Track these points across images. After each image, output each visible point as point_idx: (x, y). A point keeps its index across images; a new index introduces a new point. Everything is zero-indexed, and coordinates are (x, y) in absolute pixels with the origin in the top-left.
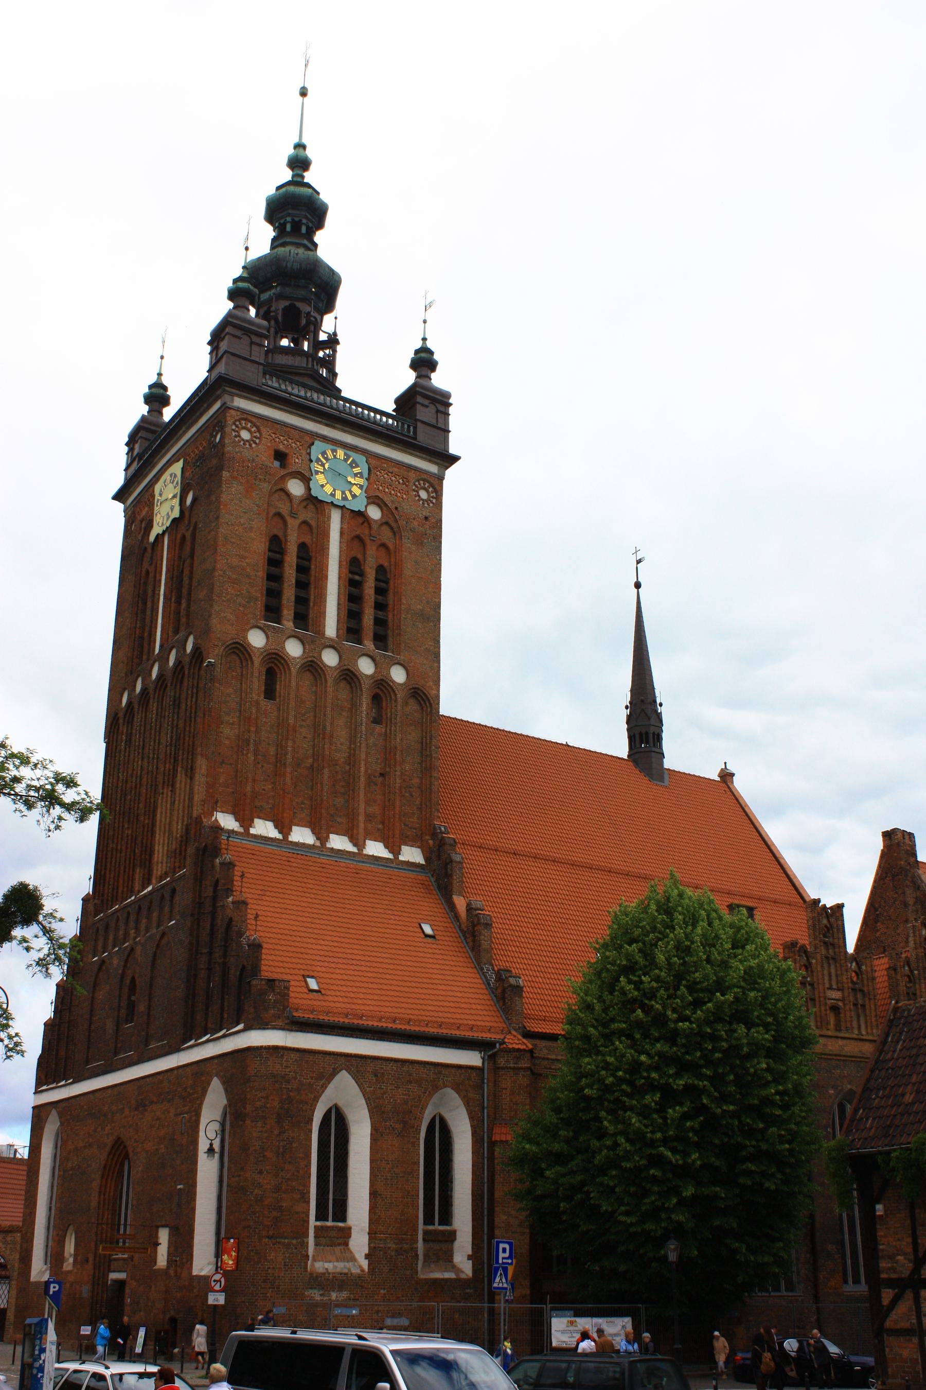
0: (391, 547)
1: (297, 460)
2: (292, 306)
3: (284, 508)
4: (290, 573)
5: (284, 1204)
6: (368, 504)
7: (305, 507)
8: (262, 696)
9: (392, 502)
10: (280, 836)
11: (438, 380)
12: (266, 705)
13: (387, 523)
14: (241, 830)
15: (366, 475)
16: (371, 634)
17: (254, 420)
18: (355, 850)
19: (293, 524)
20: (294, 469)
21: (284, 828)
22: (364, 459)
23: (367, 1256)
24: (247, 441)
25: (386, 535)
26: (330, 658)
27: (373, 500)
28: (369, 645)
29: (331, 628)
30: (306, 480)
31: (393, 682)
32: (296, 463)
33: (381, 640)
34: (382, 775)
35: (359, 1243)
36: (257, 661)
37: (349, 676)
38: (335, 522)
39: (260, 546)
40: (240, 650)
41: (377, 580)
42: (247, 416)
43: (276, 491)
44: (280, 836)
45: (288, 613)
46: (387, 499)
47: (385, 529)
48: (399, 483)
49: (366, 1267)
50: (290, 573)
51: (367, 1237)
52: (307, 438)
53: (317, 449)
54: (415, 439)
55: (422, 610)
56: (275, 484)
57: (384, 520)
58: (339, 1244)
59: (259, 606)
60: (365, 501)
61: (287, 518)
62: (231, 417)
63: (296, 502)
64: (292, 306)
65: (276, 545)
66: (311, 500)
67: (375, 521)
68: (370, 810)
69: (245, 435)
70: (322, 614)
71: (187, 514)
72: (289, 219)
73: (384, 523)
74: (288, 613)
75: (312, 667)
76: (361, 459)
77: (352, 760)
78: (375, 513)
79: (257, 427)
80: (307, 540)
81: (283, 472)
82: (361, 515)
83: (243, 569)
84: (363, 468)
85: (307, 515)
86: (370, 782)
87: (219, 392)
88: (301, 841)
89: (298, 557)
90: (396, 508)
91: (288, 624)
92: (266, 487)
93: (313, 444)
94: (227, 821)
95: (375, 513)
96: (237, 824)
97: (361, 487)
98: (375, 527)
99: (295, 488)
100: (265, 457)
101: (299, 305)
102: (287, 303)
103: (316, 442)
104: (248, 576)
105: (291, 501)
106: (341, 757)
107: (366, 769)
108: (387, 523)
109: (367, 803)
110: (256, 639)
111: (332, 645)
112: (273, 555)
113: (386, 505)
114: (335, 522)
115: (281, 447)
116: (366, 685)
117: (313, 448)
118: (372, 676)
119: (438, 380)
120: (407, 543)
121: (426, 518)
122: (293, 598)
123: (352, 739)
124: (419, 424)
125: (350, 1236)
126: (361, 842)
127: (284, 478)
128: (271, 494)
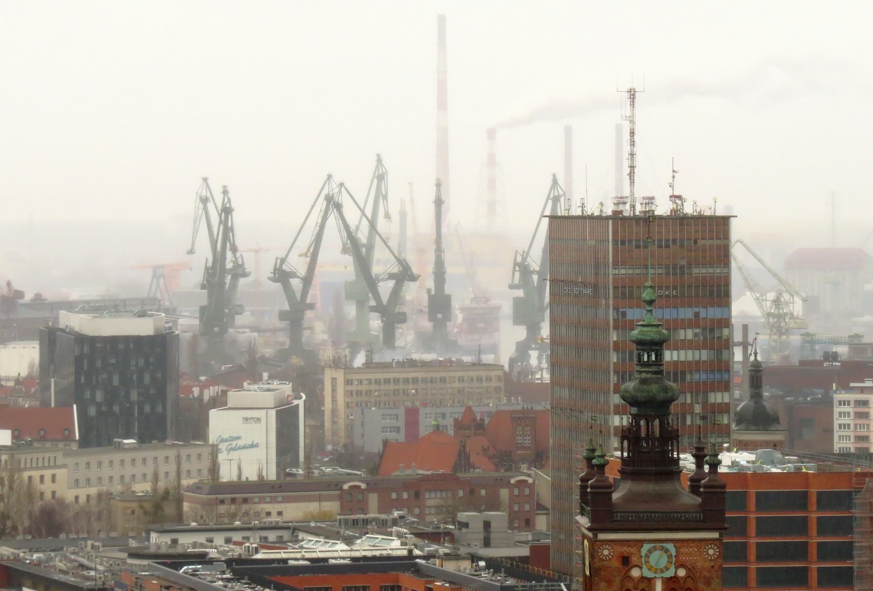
1: (634, 558)
7: (642, 582)
15: (674, 554)
20: (634, 564)
24: (607, 555)
25: (690, 584)
32: (634, 559)
43: (626, 578)
46: (688, 565)
47: (689, 580)
48: (695, 551)
56: (624, 575)
57: (687, 576)
60: (674, 570)
67: (682, 578)
73: (687, 577)
76: (671, 547)
78: (682, 573)
82: (674, 579)
84: (673, 551)
90: (694, 567)
92: (618, 580)
93: (642, 546)
95: (682, 573)
98: (682, 581)
100: (616, 564)
103: (645, 545)
105: (634, 581)
108: (689, 577)
117: (643, 548)
121: (712, 567)
127: (629, 571)
128: (622, 581)
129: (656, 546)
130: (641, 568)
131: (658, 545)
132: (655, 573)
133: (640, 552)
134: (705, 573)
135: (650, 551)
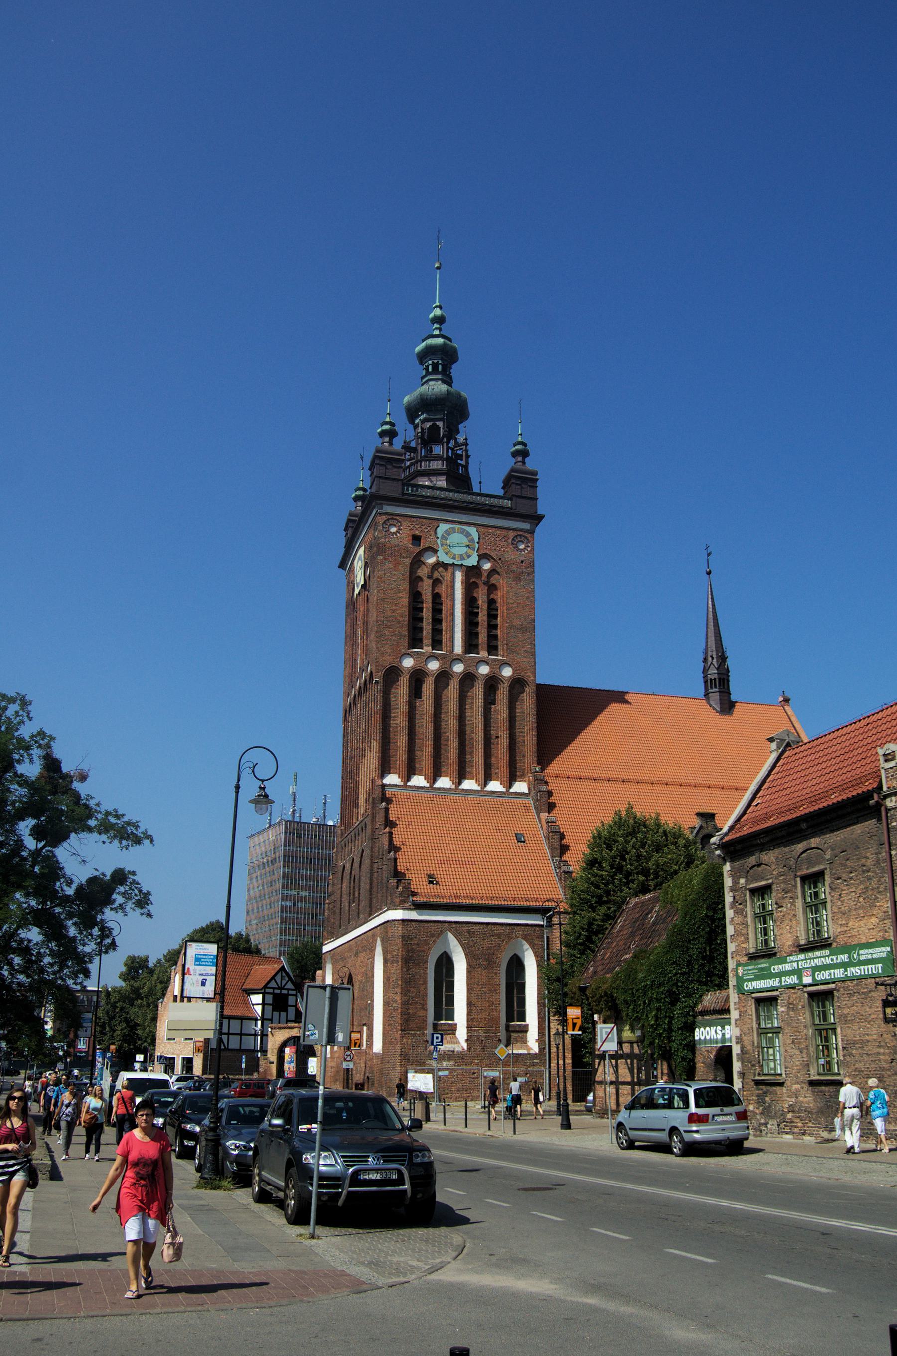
5: (410, 1011)
9: (497, 555)
10: (428, 785)
11: (531, 464)
14: (402, 783)
15: (476, 540)
18: (479, 788)
22: (475, 529)
23: (467, 1041)
28: (483, 654)
29: (458, 648)
30: (435, 551)
31: (502, 676)
33: (492, 648)
35: (462, 1033)
38: (459, 576)
39: (405, 600)
42: (392, 517)
44: (428, 785)
46: (493, 554)
49: (466, 1048)
51: (466, 1030)
52: (435, 523)
53: (443, 528)
55: (521, 625)
58: (449, 1034)
59: (405, 641)
60: (477, 559)
64: (434, 425)
65: (415, 597)
69: (393, 530)
72: (430, 362)
73: (493, 572)
76: (473, 531)
81: (418, 550)
84: (476, 537)
88: (442, 786)
90: (500, 559)
91: (427, 649)
96: (400, 780)
101: (437, 423)
104: (399, 622)
111: (459, 659)
118: (487, 675)
119: (531, 464)
121: (522, 562)
125: (456, 1030)
128: (412, 564)
129: (455, 528)
132: (454, 558)
133: (436, 533)
135: (448, 533)
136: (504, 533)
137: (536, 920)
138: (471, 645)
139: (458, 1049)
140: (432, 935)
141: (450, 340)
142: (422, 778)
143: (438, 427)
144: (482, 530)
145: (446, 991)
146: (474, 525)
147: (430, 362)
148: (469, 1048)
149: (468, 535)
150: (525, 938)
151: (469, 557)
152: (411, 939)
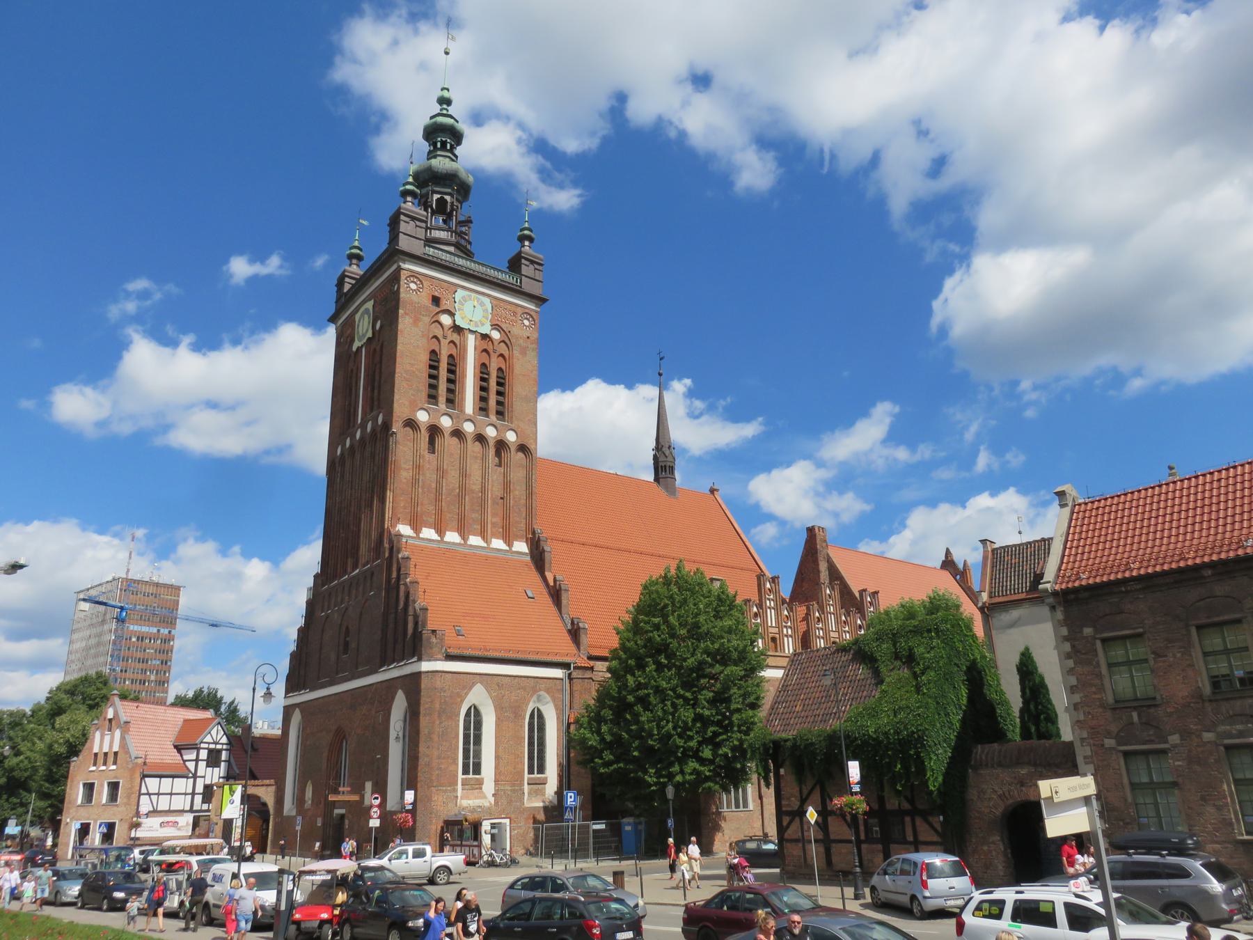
0: (507, 357)
2: (442, 198)
3: (439, 333)
4: (443, 374)
5: (443, 766)
6: (492, 329)
8: (427, 451)
12: (427, 456)
13: (503, 341)
16: (495, 412)
17: (418, 276)
18: (485, 545)
19: (444, 342)
21: (441, 532)
25: (503, 349)
26: (468, 428)
27: (495, 326)
28: (493, 418)
30: (452, 314)
32: (445, 304)
33: (500, 414)
34: (501, 498)
35: (489, 787)
36: (423, 430)
37: (480, 438)
38: (471, 341)
39: (424, 358)
40: (411, 424)
41: (498, 377)
42: (414, 275)
43: (434, 322)
44: (439, 538)
45: (442, 399)
46: (504, 326)
49: (493, 803)
50: (443, 374)
52: (453, 288)
53: (460, 294)
54: (521, 287)
61: (441, 339)
62: (403, 274)
63: (446, 329)
66: (457, 329)
68: (494, 520)
69: (413, 286)
70: (463, 399)
71: (377, 335)
72: (439, 139)
74: (442, 399)
75: (458, 433)
76: (487, 301)
77: (483, 489)
78: (496, 335)
79: (421, 281)
80: (454, 352)
82: (485, 337)
83: (414, 372)
85: (455, 337)
86: (494, 503)
87: (396, 258)
89: (448, 364)
91: (442, 405)
94: (405, 530)
95: (496, 335)
97: (487, 319)
98: (496, 343)
99: (446, 320)
100: (427, 302)
102: (439, 196)
106: (477, 487)
107: (492, 495)
109: (492, 517)
110: (422, 417)
112: (432, 363)
113: (504, 331)
114: (471, 341)
115: (436, 294)
116: (492, 443)
120: (516, 353)
122: (445, 390)
123: (483, 477)
124: (523, 277)
125: (482, 784)
126: (489, 540)
130: (452, 314)
131: (473, 295)
134: (521, 341)
136: (513, 308)
137: (558, 673)
138: (483, 410)
139: (487, 804)
140: (464, 688)
141: (457, 122)
142: (433, 531)
143: (446, 201)
144: (495, 302)
145: (474, 745)
146: (489, 296)
147: (439, 139)
148: (496, 802)
149: (482, 304)
150: (548, 691)
151: (483, 324)
152: (445, 691)
